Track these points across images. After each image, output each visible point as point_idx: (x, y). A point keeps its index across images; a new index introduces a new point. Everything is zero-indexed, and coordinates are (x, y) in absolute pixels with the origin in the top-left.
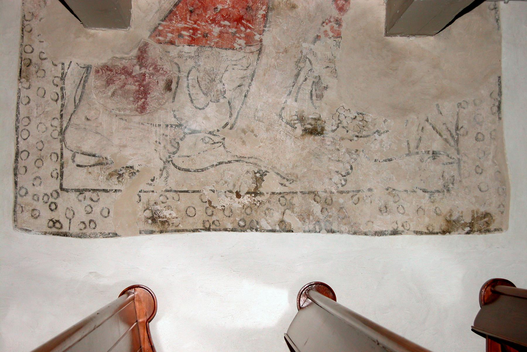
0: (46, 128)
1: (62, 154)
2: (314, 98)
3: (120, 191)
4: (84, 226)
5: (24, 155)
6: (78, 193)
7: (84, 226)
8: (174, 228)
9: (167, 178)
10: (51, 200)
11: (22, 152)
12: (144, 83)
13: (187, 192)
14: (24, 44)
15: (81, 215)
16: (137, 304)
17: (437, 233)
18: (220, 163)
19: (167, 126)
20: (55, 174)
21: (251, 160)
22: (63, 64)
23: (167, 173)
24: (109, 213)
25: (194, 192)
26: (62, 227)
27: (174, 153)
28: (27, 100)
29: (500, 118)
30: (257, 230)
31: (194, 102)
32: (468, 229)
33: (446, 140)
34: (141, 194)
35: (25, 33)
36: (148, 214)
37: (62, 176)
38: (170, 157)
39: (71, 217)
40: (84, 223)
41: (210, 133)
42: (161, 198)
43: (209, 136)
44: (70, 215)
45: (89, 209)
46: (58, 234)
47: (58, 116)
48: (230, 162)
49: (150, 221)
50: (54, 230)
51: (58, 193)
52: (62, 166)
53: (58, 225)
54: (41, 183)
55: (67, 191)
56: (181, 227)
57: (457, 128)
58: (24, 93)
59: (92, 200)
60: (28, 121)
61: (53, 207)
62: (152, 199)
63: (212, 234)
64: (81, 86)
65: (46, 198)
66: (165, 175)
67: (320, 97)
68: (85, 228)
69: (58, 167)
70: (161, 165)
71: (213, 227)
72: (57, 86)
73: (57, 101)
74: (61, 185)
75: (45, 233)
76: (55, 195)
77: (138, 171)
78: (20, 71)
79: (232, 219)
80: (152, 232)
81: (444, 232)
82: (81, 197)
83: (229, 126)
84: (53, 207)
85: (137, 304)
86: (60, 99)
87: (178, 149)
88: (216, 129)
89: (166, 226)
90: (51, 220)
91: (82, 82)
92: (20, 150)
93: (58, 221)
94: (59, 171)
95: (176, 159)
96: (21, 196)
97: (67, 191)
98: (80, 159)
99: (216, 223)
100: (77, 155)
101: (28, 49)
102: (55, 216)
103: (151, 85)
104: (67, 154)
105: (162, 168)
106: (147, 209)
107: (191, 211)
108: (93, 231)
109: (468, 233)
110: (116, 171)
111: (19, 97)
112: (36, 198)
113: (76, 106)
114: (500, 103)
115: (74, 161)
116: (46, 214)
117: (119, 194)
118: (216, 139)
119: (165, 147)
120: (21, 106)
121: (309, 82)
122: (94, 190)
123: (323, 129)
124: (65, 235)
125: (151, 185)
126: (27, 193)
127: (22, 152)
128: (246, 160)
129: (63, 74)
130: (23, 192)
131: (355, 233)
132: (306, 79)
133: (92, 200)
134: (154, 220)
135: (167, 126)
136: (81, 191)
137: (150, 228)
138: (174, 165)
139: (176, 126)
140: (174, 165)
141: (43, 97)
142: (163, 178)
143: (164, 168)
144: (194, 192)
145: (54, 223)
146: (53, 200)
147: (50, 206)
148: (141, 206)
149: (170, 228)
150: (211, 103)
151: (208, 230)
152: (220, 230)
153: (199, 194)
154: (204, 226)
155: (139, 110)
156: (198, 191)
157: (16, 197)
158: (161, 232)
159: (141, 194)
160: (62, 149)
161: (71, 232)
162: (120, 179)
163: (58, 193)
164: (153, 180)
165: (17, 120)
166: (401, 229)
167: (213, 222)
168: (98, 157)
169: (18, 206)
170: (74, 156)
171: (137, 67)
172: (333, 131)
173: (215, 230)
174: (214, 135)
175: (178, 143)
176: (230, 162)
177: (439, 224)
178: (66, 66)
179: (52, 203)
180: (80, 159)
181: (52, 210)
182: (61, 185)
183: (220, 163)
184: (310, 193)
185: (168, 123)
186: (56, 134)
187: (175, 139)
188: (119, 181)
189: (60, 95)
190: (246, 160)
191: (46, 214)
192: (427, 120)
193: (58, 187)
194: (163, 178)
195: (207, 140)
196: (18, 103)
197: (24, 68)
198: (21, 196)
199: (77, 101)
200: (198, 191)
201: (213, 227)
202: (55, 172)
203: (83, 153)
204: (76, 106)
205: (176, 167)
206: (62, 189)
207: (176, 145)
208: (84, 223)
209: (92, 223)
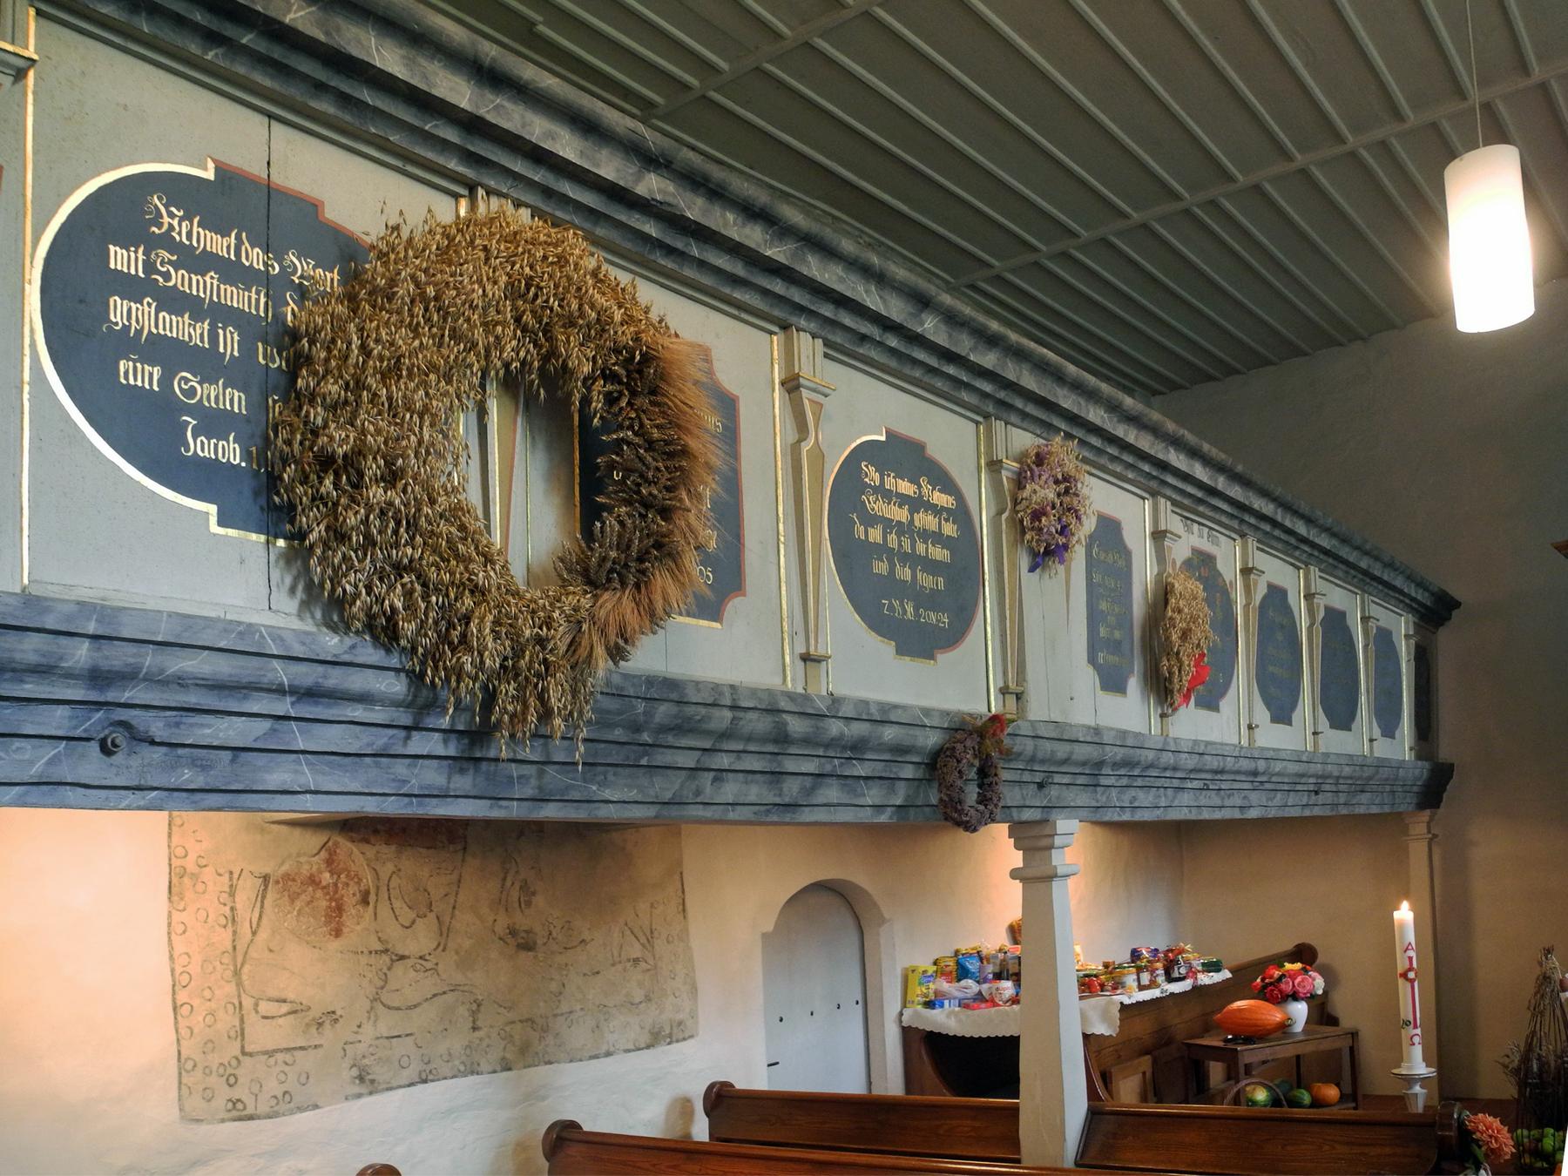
0: (214, 968)
1: (240, 1003)
2: (523, 906)
3: (321, 1046)
4: (276, 1101)
5: (185, 1010)
6: (266, 1056)
7: (276, 1101)
8: (385, 1086)
9: (375, 1022)
10: (230, 1071)
11: (182, 1005)
12: (337, 896)
13: (399, 1036)
14: (173, 845)
15: (273, 1087)
16: (492, 183)
17: (642, 1049)
18: (435, 995)
19: (371, 952)
20: (233, 1034)
21: (466, 988)
22: (231, 873)
23: (376, 1016)
24: (308, 1078)
25: (407, 1035)
26: (245, 1108)
27: (382, 988)
28: (183, 928)
30: (478, 1074)
31: (399, 918)
32: (668, 1040)
33: (643, 945)
34: (346, 1047)
35: (173, 828)
36: (355, 1072)
37: (243, 1034)
38: (377, 994)
39: (257, 1092)
40: (275, 1097)
41: (421, 958)
42: (371, 1049)
43: (420, 961)
44: (256, 1089)
45: (282, 1077)
46: (240, 1119)
47: (230, 948)
48: (444, 993)
49: (357, 1081)
50: (235, 1114)
51: (237, 1059)
52: (242, 1020)
53: (240, 1106)
54: (214, 1048)
55: (251, 1055)
56: (394, 1084)
57: (652, 932)
58: (177, 916)
59: (286, 1064)
60: (188, 960)
61: (232, 1080)
62: (359, 1052)
63: (431, 1085)
64: (258, 904)
65: (221, 1070)
66: (373, 1018)
67: (529, 904)
68: (277, 1104)
69: (237, 1024)
70: (367, 1005)
71: (430, 1077)
72: (225, 905)
73: (225, 927)
74: (243, 1047)
75: (223, 1121)
76: (234, 1063)
77: (341, 1016)
78: (170, 887)
79: (450, 1064)
80: (359, 1096)
81: (648, 1047)
82: (272, 1061)
83: (441, 948)
84: (232, 1080)
85: (492, 183)
86: (230, 925)
87: (386, 982)
88: (427, 952)
89: (376, 1085)
90: (230, 1100)
91: (259, 899)
92: (179, 1003)
93: (238, 1100)
94: (238, 1029)
95: (385, 997)
96: (188, 1072)
97: (251, 1055)
98: (264, 1007)
99: (434, 1072)
100: (261, 1002)
101: (179, 852)
102: (237, 1093)
103: (345, 899)
104: (248, 1003)
105: (369, 1008)
106: (354, 1065)
107: (405, 1061)
108: (288, 1106)
109: (669, 1044)
110: (314, 1019)
111: (169, 924)
112: (207, 1071)
113: (254, 933)
115: (257, 1012)
116: (224, 1093)
117: (320, 1051)
118: (429, 965)
119: (370, 981)
120: (173, 936)
121: (517, 886)
122: (288, 1050)
123: (535, 943)
124: (251, 1118)
125: (356, 1033)
126: (195, 1066)
127: (182, 1005)
128: (461, 988)
129: (231, 886)
130: (189, 1065)
131: (571, 1061)
132: (513, 884)
133: (286, 1064)
134: (361, 1078)
135: (371, 952)
136: (270, 1054)
137: (357, 1089)
138: (382, 1003)
139: (382, 952)
140: (382, 1003)
141: (205, 922)
142: (371, 1022)
143: (372, 1008)
144: (407, 1035)
145: (234, 1104)
146: (233, 1072)
147: (227, 1080)
148: (346, 1063)
149: (380, 1087)
150: (418, 920)
151: (425, 1081)
152: (438, 1080)
153: (413, 1037)
154: (420, 1078)
155: (333, 933)
156: (411, 1035)
157: (180, 1074)
158: (371, 1093)
159: (346, 1047)
160: (239, 996)
161: (258, 1112)
162: (320, 1030)
163: (237, 1059)
164: (359, 1026)
165: (171, 957)
166: (612, 1049)
167: (430, 1072)
168: (291, 1002)
169: (183, 1087)
170: (256, 1005)
171: (327, 875)
172: (545, 944)
173: (432, 1081)
174: (426, 960)
175: (385, 974)
176: (444, 993)
177: (644, 1038)
178: (236, 876)
179: (230, 1075)
180: (264, 1007)
181: (231, 1086)
182: (243, 1047)
183: (435, 995)
184: (528, 1020)
185: (372, 949)
186: (229, 974)
187: (381, 970)
188: (319, 1033)
189: (230, 919)
190: (461, 988)
191: (224, 1093)
192: (626, 924)
193: (237, 1052)
194: (371, 1022)
195: (418, 967)
196: (169, 933)
197: (175, 880)
198: (188, 1072)
199: (254, 926)
200: (411, 1035)
201: (430, 1077)
202: (234, 1029)
203: (269, 1000)
204: (254, 933)
205: (384, 1006)
206: (244, 1053)
207: (383, 977)
208: (275, 1097)
209: (287, 1096)
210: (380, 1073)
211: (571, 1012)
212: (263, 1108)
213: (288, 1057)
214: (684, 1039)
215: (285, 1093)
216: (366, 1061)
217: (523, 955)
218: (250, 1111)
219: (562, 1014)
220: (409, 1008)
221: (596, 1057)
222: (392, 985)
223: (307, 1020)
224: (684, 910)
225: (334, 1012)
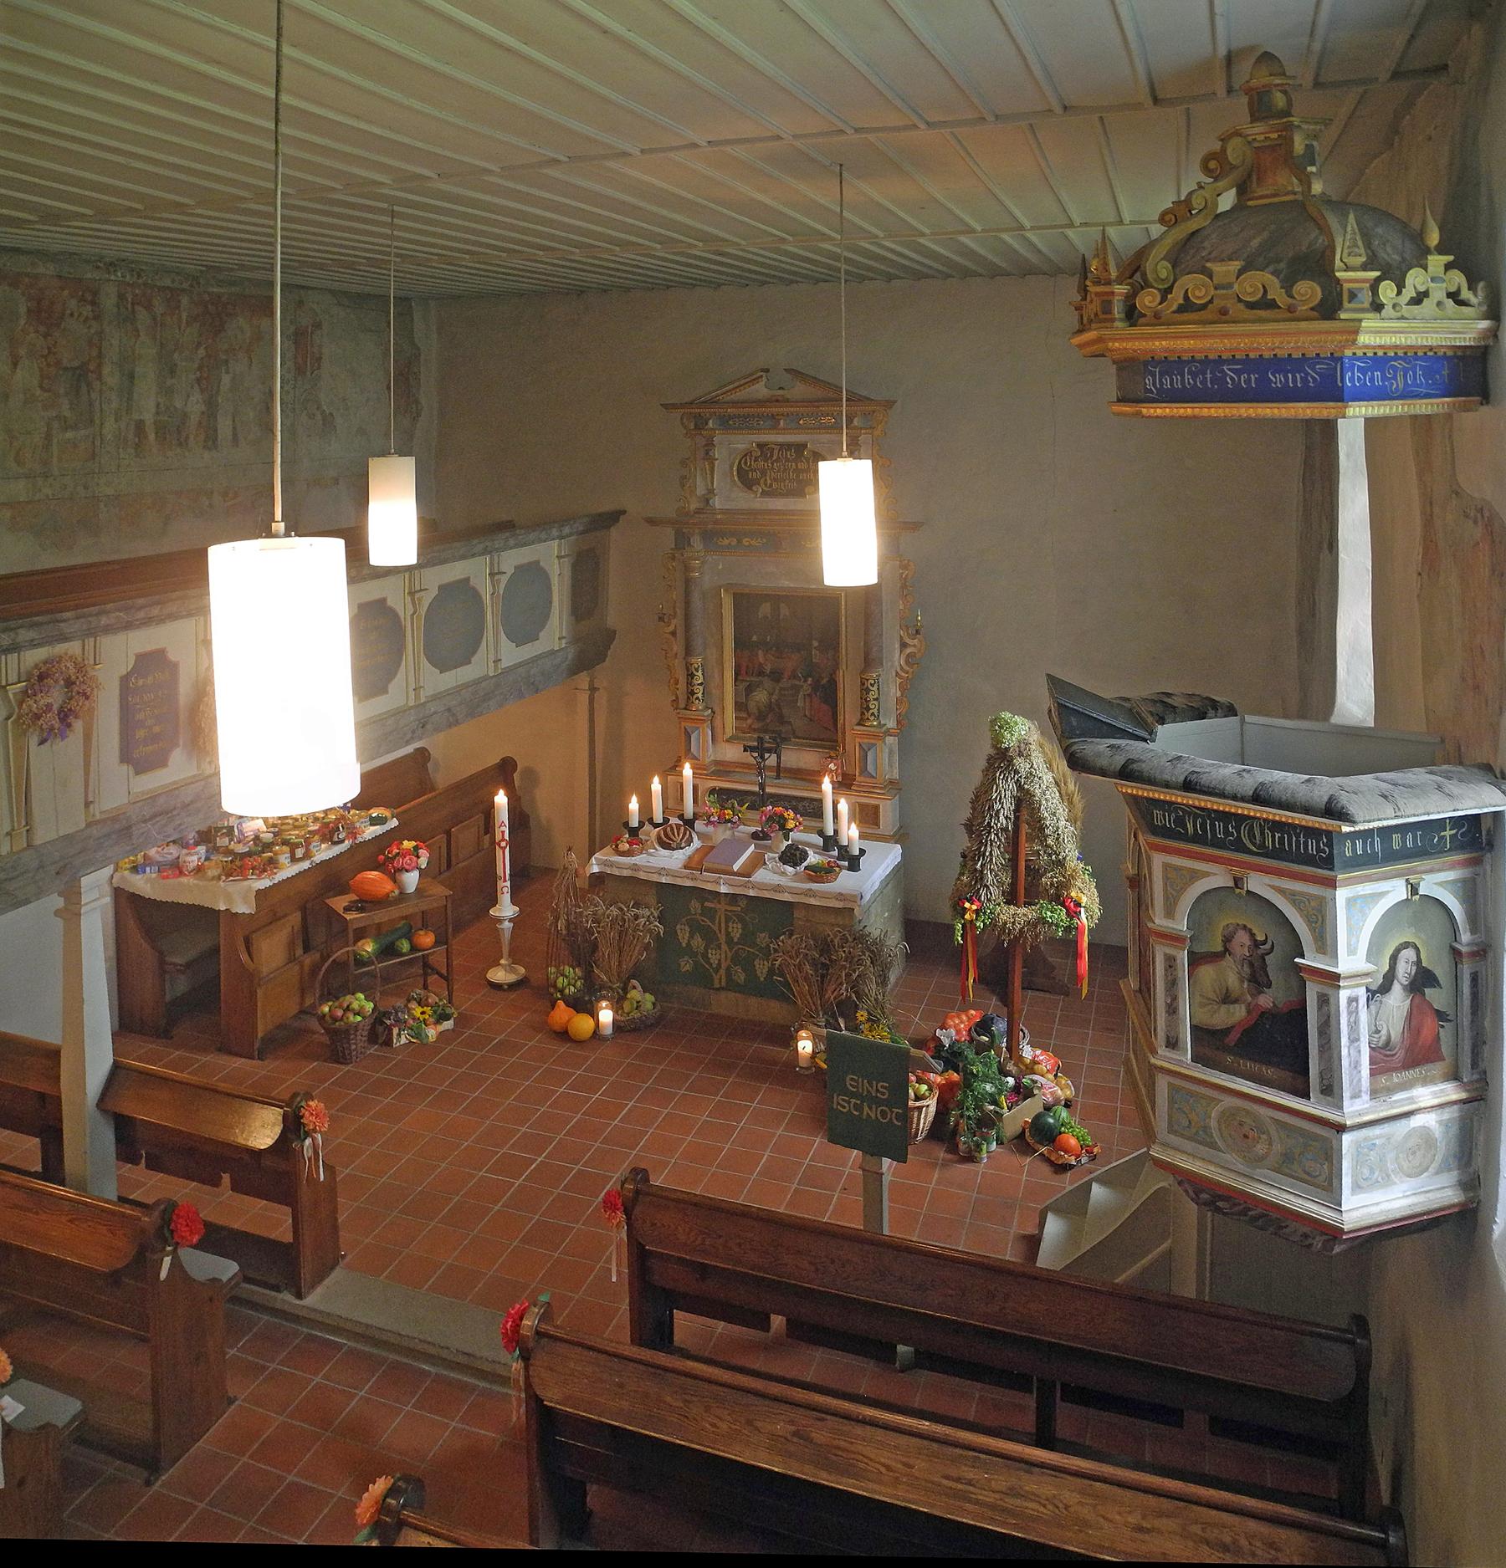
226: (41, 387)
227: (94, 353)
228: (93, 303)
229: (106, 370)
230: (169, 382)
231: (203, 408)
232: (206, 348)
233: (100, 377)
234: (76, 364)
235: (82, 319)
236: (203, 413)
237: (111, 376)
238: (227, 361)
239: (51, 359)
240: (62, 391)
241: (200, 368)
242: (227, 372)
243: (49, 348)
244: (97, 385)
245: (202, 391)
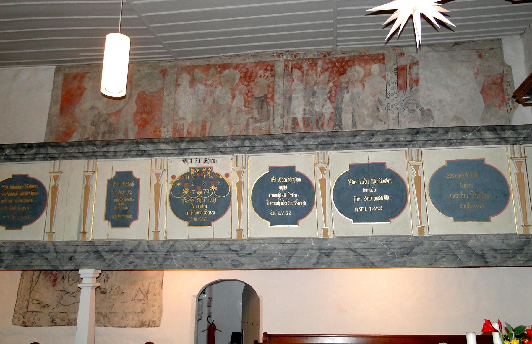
5: (18, 300)
10: (24, 315)
18: (74, 303)
26: (26, 324)
29: (162, 288)
32: (147, 326)
33: (144, 295)
36: (51, 320)
50: (24, 325)
53: (25, 323)
55: (29, 312)
57: (148, 291)
66: (57, 307)
67: (107, 281)
69: (27, 304)
71: (70, 324)
75: (21, 326)
80: (52, 326)
93: (25, 322)
95: (62, 302)
97: (29, 312)
98: (35, 302)
102: (25, 320)
104: (31, 300)
109: (148, 327)
111: (20, 281)
113: (35, 284)
114: (162, 282)
116: (22, 320)
123: (106, 292)
124: (26, 326)
130: (16, 312)
131: (113, 327)
134: (53, 321)
136: (33, 312)
145: (24, 322)
151: (68, 325)
154: (67, 323)
158: (55, 326)
159: (50, 313)
166: (127, 326)
170: (32, 300)
172: (109, 292)
180: (35, 302)
181: (24, 318)
183: (74, 303)
191: (22, 320)
193: (26, 311)
204: (35, 284)
205: (61, 304)
206: (27, 311)
210: (58, 321)
211: (115, 312)
212: (29, 325)
213: (36, 314)
214: (154, 327)
215: (34, 322)
216: (54, 317)
217: (102, 295)
218: (26, 325)
219: (112, 313)
220: (67, 306)
221: (121, 327)
222: (64, 299)
223: (42, 305)
224: (162, 286)
225: (48, 304)
226: (245, 106)
227: (270, 90)
228: (272, 70)
229: (276, 97)
230: (311, 100)
231: (332, 110)
232: (334, 83)
233: (273, 100)
234: (261, 95)
235: (265, 77)
236: (332, 113)
237: (278, 99)
238: (347, 88)
239: (249, 95)
240: (254, 107)
241: (330, 92)
242: (348, 93)
243: (248, 90)
244: (271, 103)
245: (332, 102)
